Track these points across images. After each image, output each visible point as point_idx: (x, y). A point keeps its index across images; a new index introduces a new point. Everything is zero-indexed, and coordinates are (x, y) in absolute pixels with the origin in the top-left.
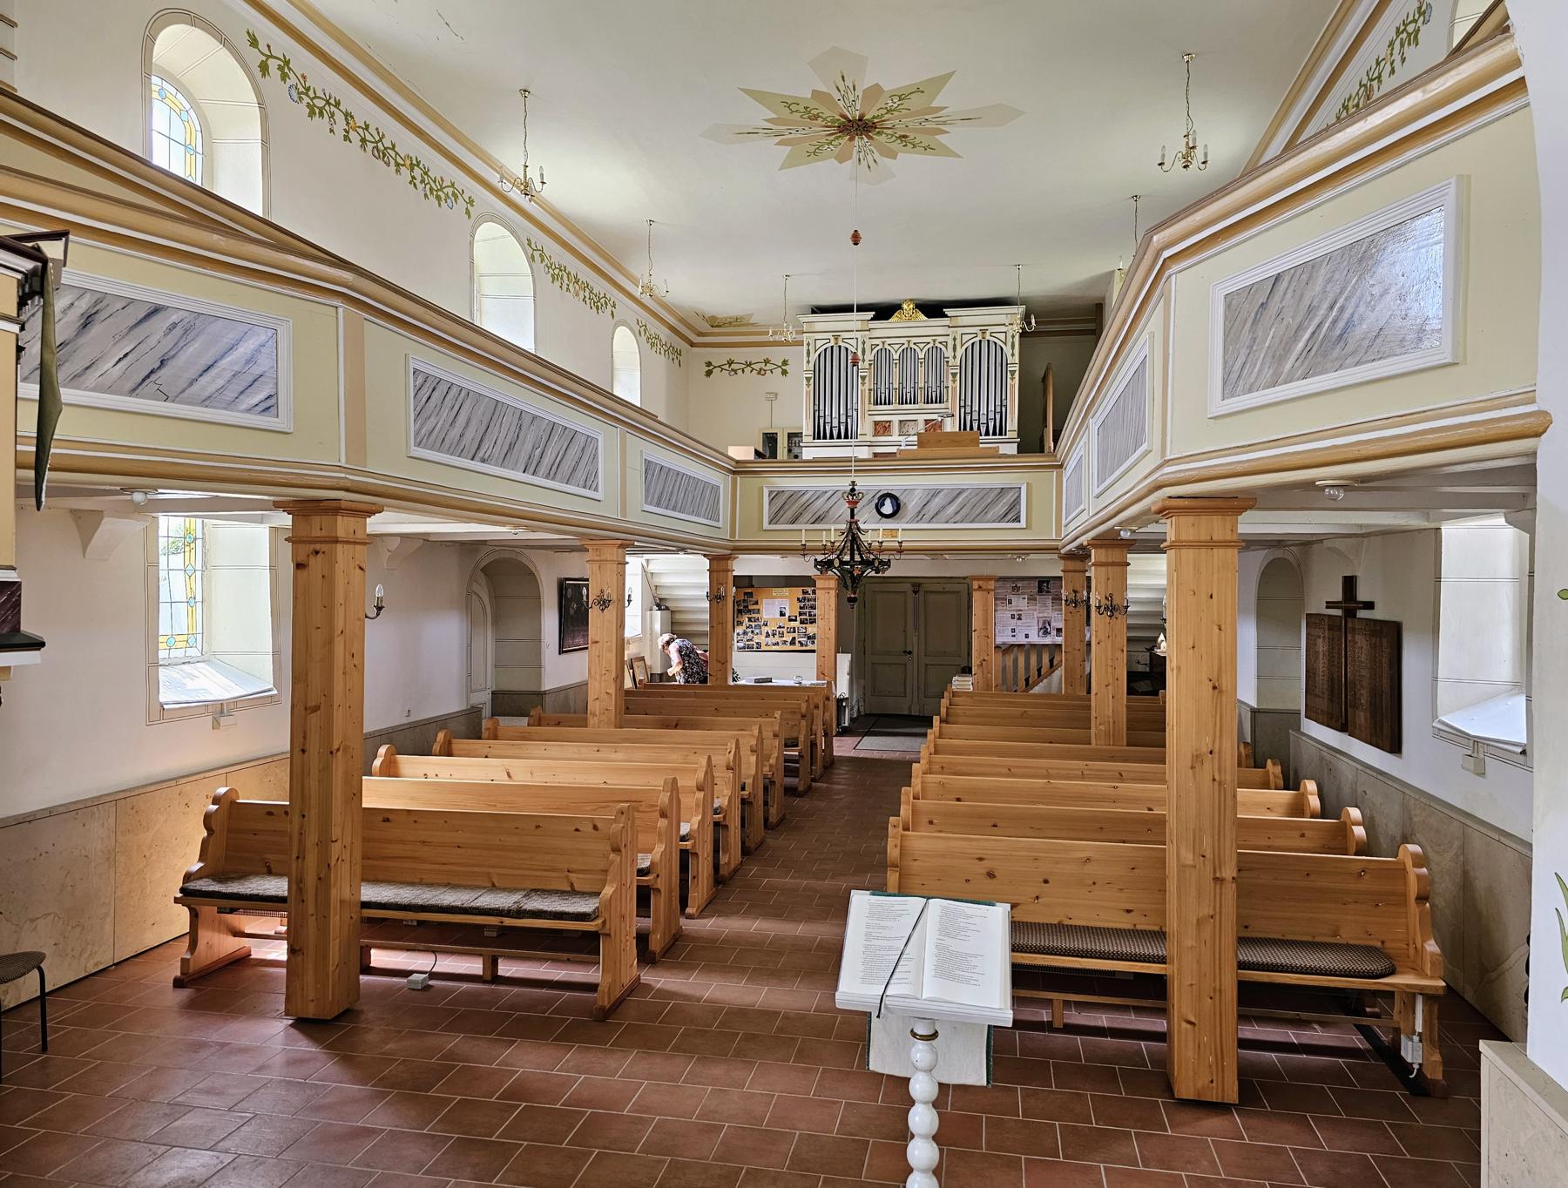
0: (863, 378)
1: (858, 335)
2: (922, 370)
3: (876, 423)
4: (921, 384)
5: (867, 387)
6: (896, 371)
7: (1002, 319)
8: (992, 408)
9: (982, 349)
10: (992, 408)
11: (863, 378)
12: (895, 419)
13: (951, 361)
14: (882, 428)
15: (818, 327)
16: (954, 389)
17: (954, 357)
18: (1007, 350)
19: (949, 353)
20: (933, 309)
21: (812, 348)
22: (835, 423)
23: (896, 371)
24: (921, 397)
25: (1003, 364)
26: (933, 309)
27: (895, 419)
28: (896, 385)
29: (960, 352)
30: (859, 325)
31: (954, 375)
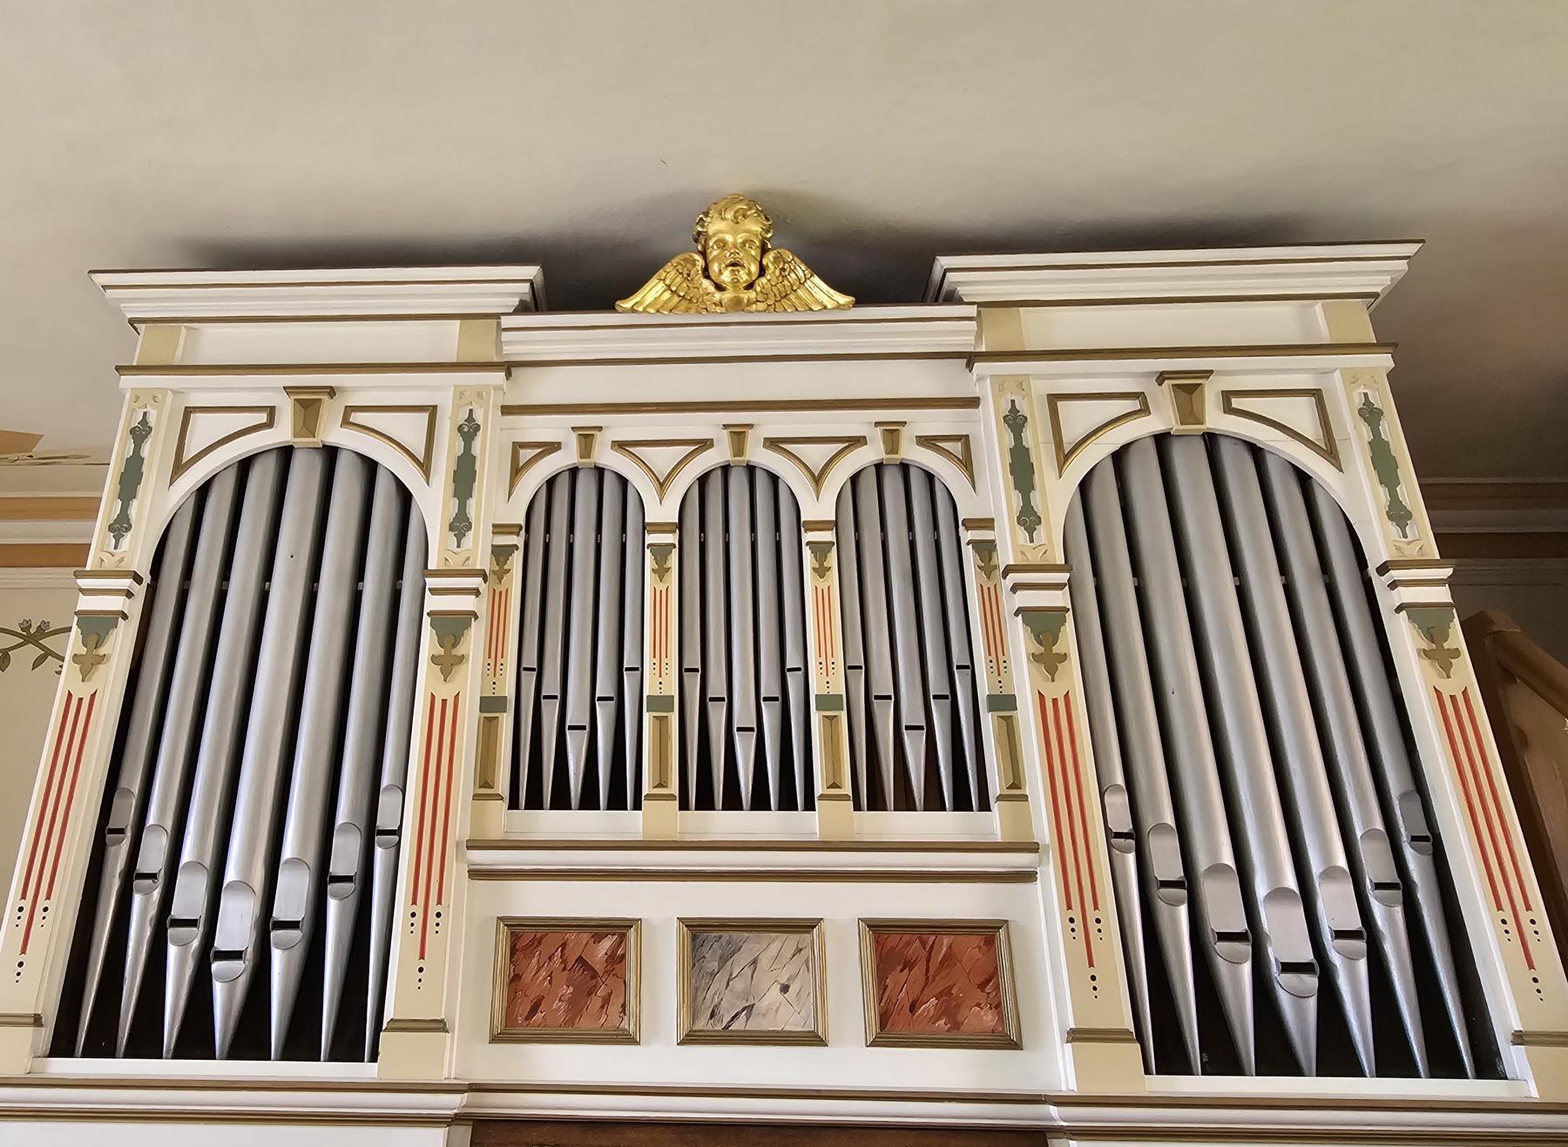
0: (452, 627)
1: (441, 389)
2: (822, 591)
3: (524, 939)
4: (827, 678)
5: (470, 684)
6: (659, 592)
7: (1278, 322)
8: (1326, 851)
9: (1179, 480)
10: (1326, 851)
11: (452, 627)
12: (659, 910)
13: (1009, 544)
14: (565, 977)
15: (217, 343)
16: (1052, 713)
17: (1019, 525)
18: (1353, 489)
19: (988, 495)
20: (887, 268)
21: (156, 454)
22: (237, 928)
23: (659, 592)
24: (830, 763)
25: (1343, 574)
26: (887, 268)
27: (659, 910)
28: (660, 678)
29: (1057, 494)
30: (447, 341)
31: (1042, 623)
